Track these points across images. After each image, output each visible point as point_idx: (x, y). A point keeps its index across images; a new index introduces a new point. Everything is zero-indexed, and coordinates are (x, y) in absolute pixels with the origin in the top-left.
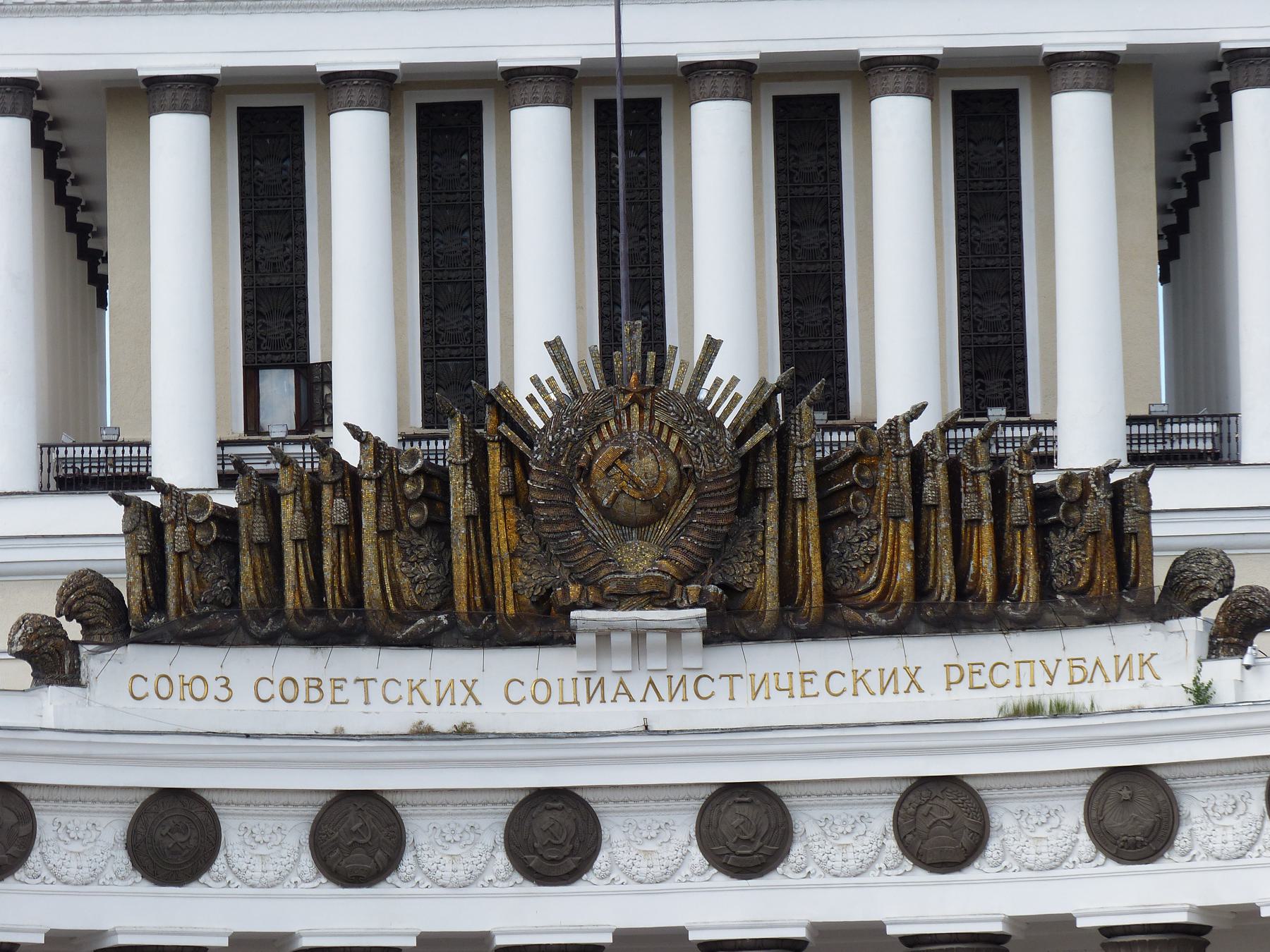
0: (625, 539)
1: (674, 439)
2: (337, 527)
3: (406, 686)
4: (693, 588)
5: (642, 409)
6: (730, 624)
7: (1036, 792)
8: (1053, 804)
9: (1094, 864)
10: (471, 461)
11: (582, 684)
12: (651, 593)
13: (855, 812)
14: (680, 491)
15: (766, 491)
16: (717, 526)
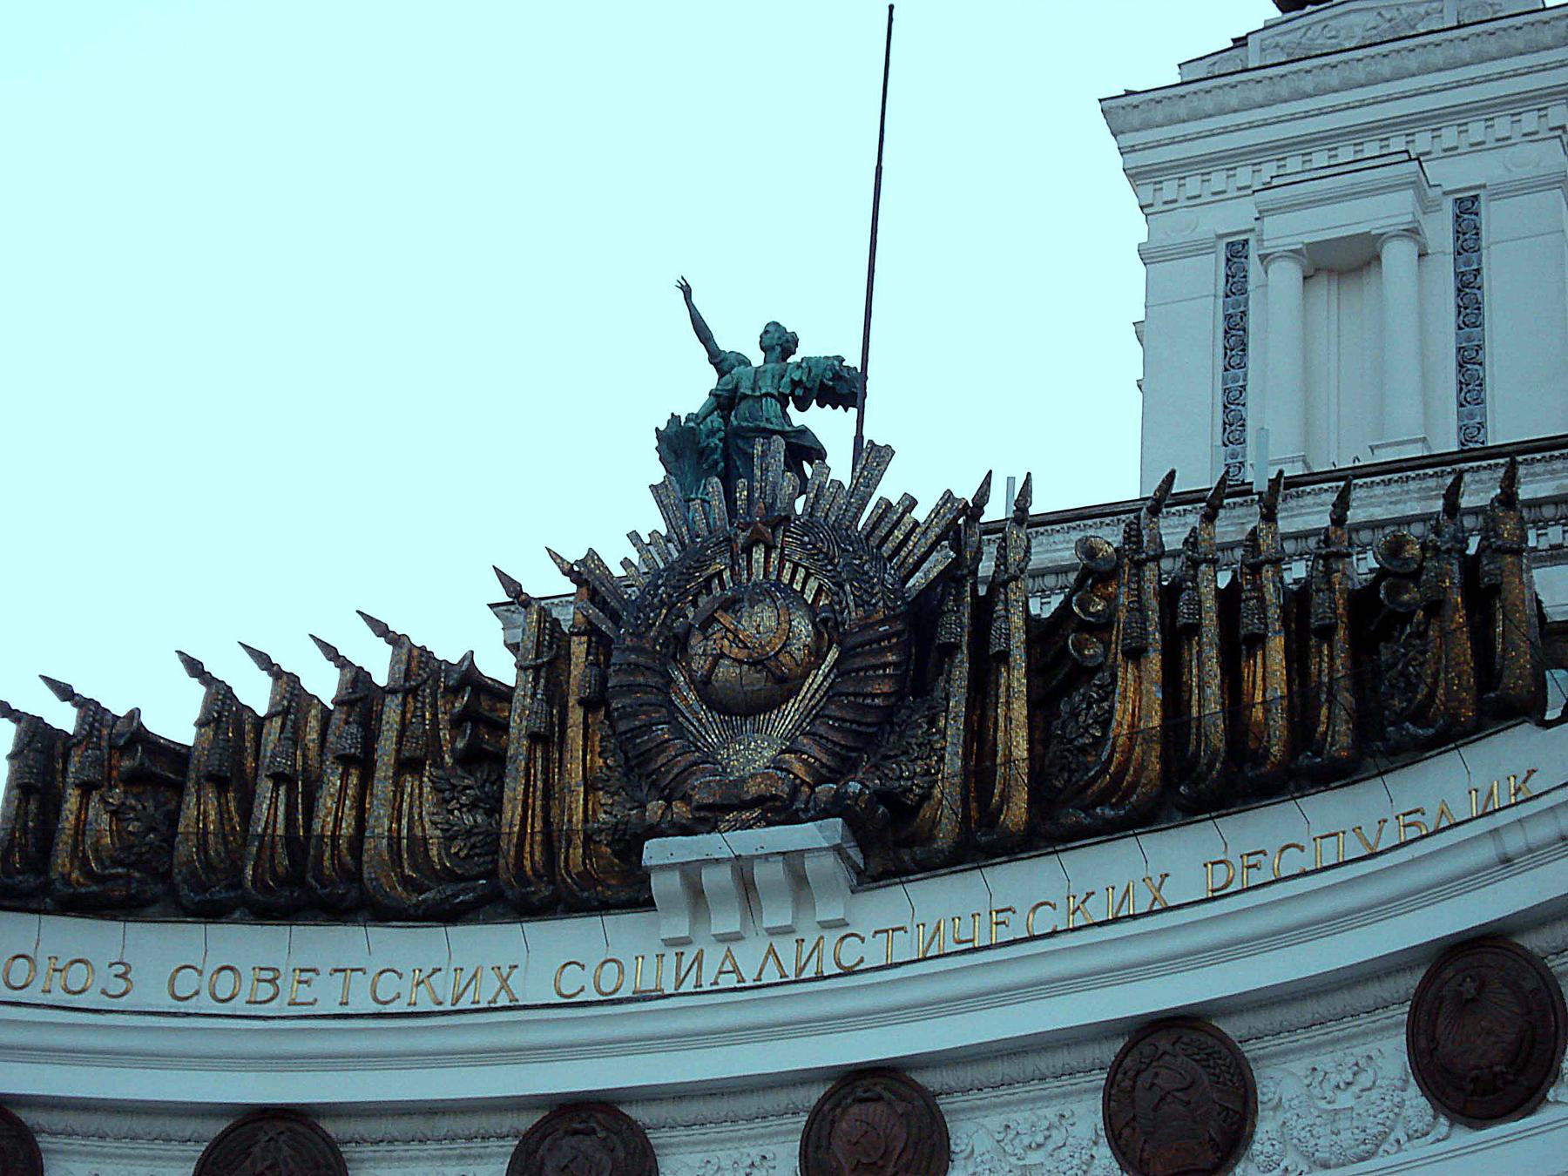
0: (735, 734)
1: (813, 584)
2: (346, 760)
3: (408, 976)
4: (826, 790)
5: (768, 551)
6: (892, 846)
7: (1335, 1029)
8: (1359, 1051)
9: (1430, 1138)
10: (550, 663)
11: (670, 959)
12: (759, 801)
13: (1051, 1113)
14: (818, 655)
15: (951, 649)
16: (866, 696)
